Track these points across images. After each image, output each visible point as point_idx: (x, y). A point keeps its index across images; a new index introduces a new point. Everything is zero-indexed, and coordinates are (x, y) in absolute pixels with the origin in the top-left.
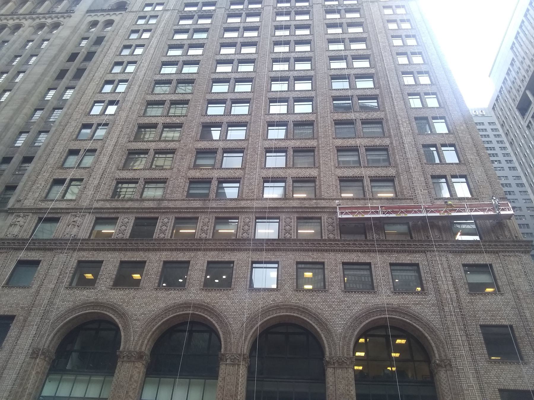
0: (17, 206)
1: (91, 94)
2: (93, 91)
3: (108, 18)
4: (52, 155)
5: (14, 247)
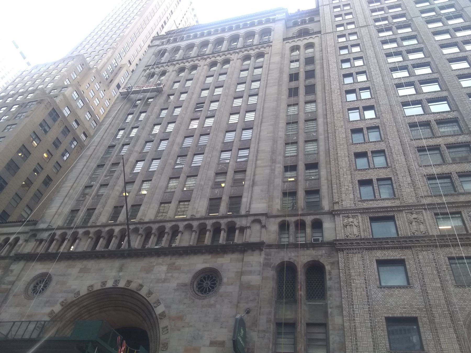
0: (336, 207)
1: (340, 103)
2: (340, 100)
3: (306, 42)
4: (340, 159)
5: (365, 246)
